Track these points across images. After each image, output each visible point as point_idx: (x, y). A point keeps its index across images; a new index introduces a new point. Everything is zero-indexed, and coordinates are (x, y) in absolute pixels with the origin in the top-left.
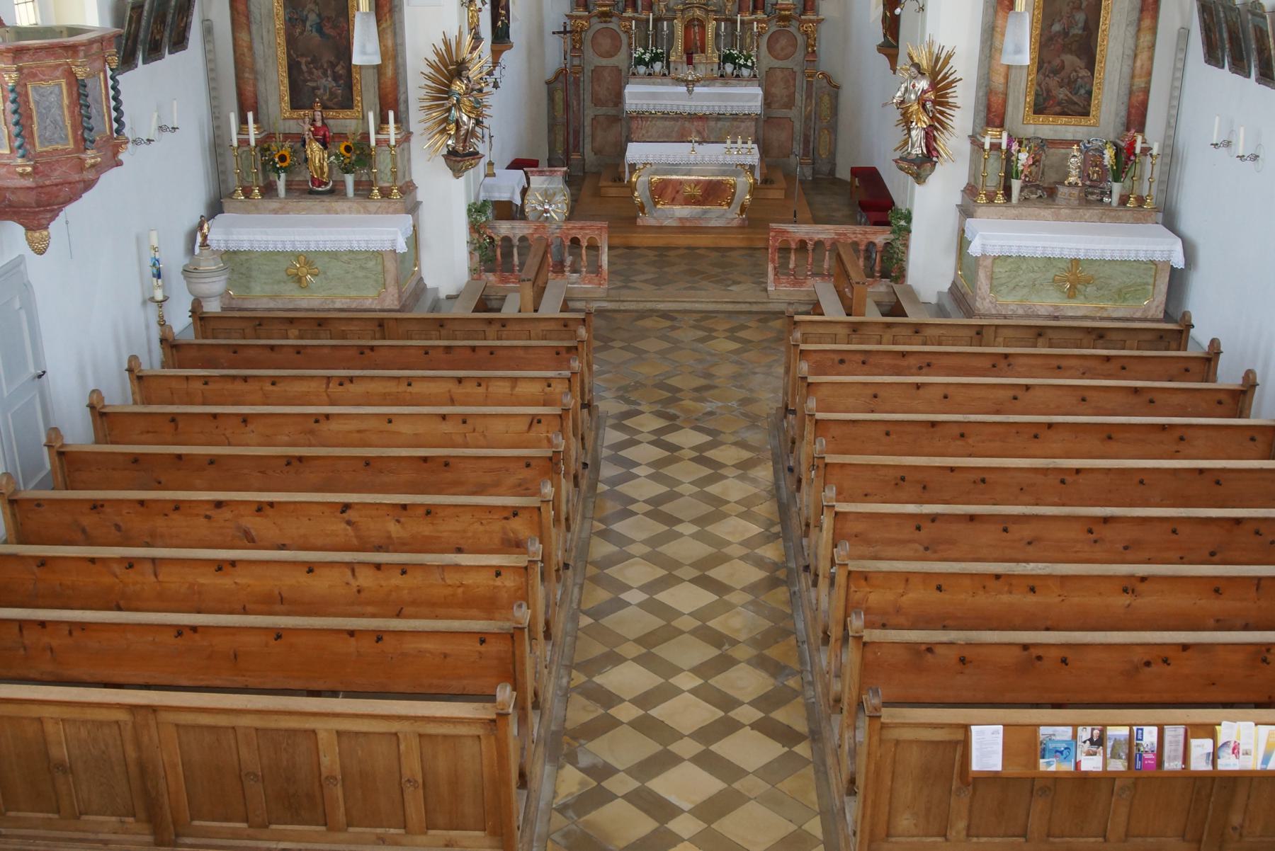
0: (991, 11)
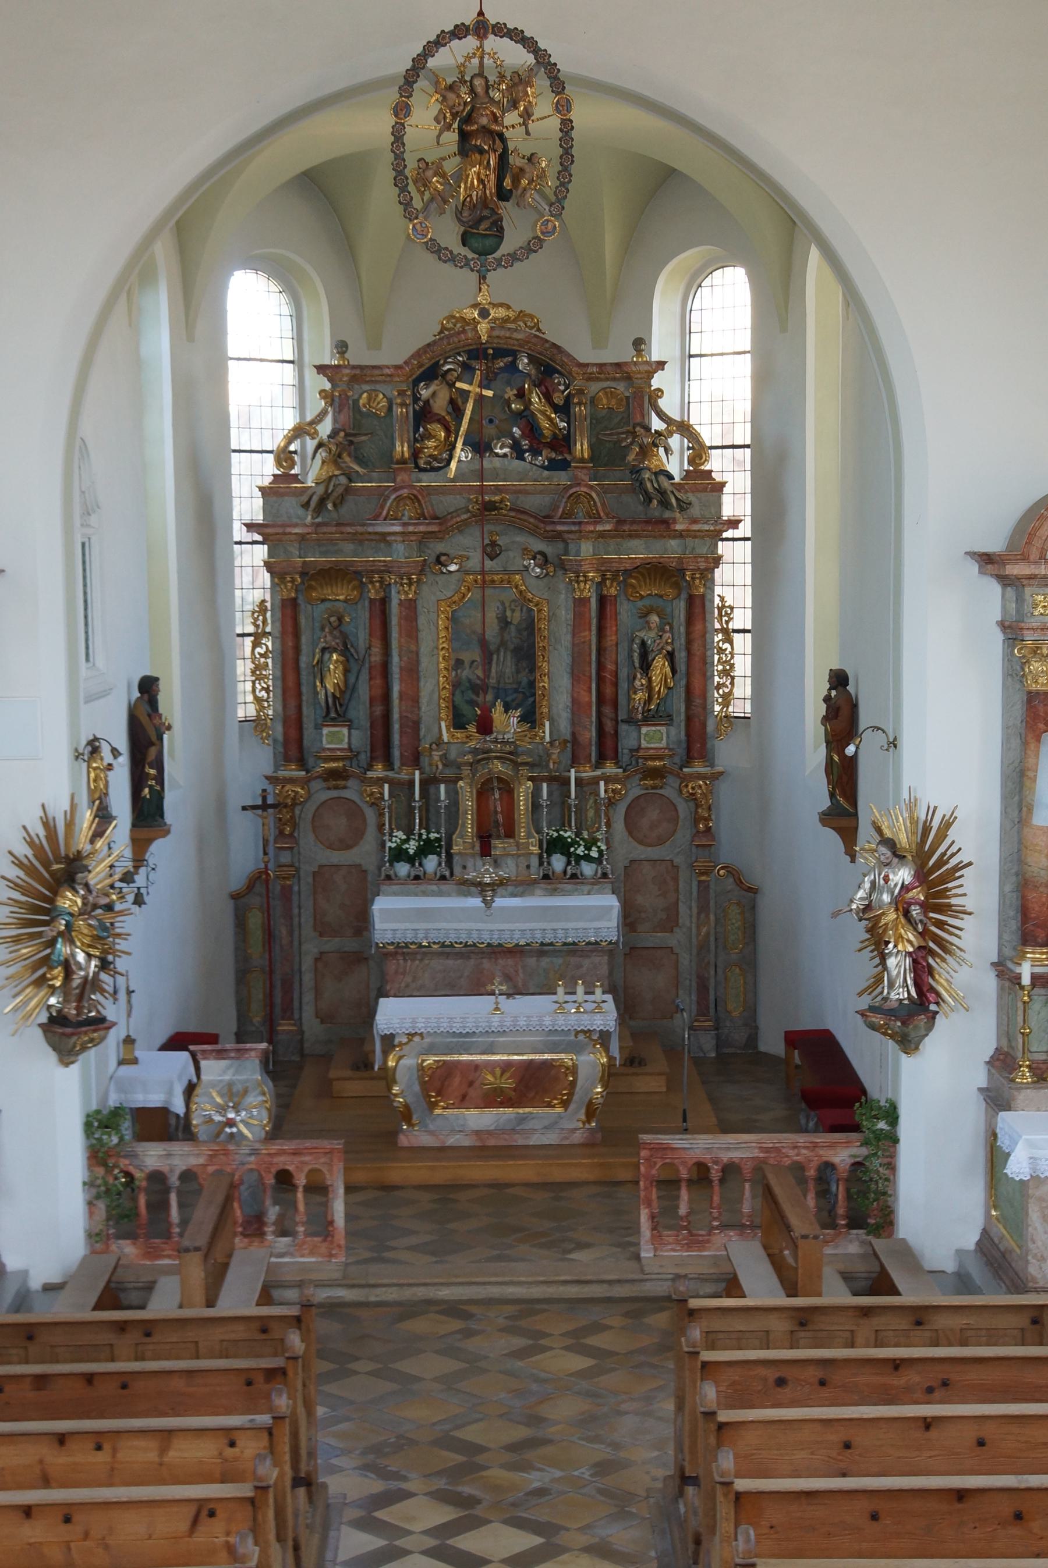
0: (1016, 742)
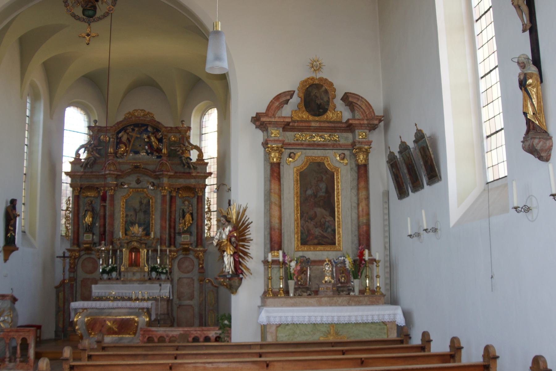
0: (268, 183)
